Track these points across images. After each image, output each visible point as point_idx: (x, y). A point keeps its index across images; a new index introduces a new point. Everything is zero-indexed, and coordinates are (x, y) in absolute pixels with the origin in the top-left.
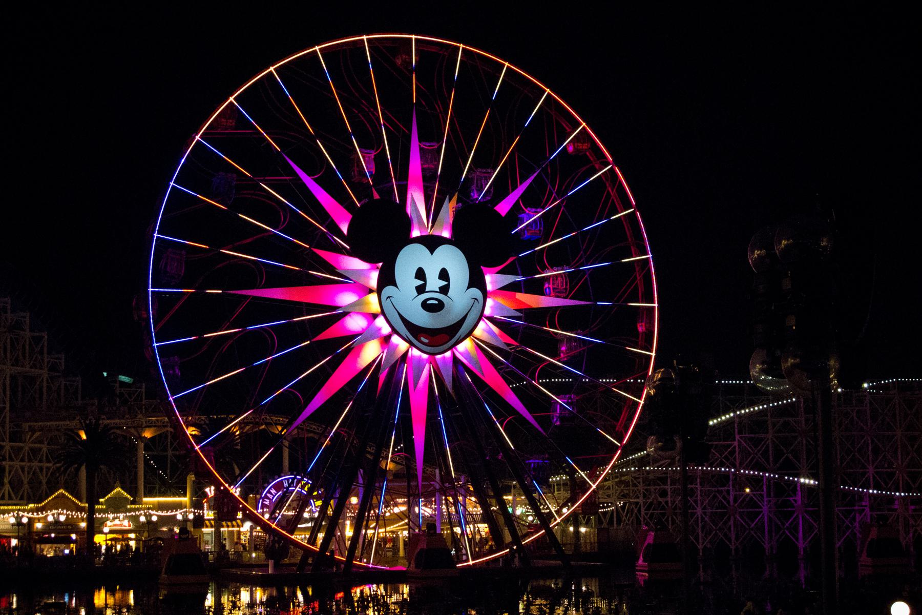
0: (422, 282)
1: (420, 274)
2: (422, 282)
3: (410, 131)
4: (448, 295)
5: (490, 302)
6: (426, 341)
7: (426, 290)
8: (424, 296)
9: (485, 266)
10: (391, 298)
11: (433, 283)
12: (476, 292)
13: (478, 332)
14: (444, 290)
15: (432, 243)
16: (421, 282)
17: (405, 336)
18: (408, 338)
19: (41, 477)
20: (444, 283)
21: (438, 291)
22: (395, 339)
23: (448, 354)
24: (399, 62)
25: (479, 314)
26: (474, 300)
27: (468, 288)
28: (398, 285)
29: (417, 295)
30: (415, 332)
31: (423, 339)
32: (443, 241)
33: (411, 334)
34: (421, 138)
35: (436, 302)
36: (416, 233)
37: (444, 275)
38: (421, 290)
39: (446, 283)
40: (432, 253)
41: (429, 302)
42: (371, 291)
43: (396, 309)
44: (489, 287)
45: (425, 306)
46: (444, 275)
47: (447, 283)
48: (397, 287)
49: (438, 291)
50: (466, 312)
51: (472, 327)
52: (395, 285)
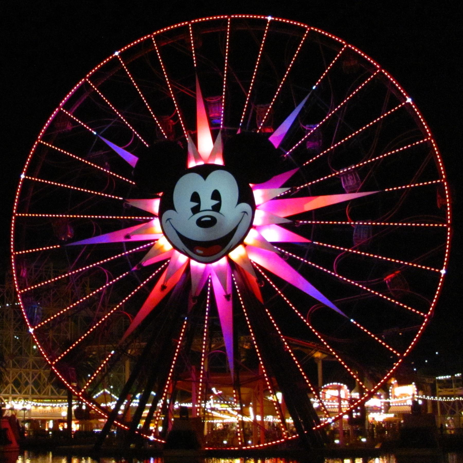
0: (196, 204)
7: (201, 209)
8: (198, 215)
10: (170, 220)
12: (245, 206)
13: (246, 241)
14: (217, 208)
16: (195, 204)
17: (183, 250)
18: (185, 251)
20: (215, 202)
21: (211, 208)
22: (177, 252)
23: (223, 261)
25: (249, 224)
26: (243, 213)
29: (192, 214)
33: (188, 248)
36: (192, 164)
37: (216, 195)
38: (196, 210)
42: (154, 216)
43: (173, 226)
45: (200, 223)
50: (237, 224)
51: (242, 236)
52: (173, 208)
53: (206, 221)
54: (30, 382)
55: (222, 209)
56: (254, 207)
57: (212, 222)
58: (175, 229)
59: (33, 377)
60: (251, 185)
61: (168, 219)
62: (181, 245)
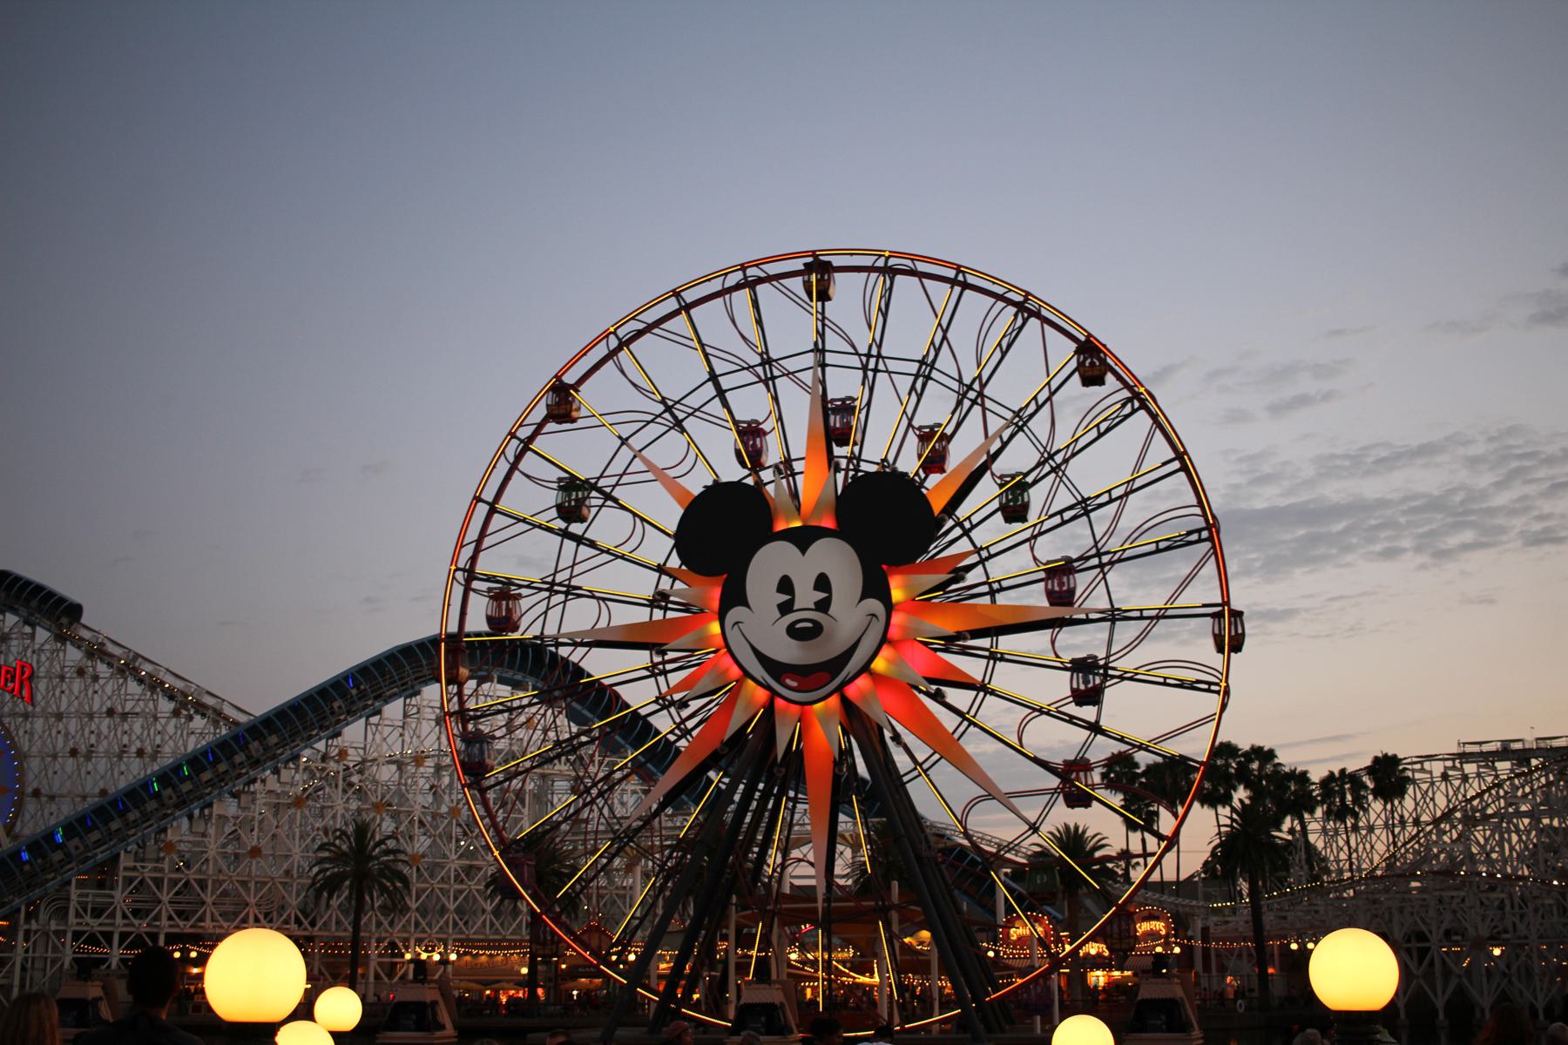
0: (787, 597)
1: (785, 585)
2: (786, 597)
4: (831, 612)
5: (897, 619)
6: (794, 684)
7: (795, 608)
9: (890, 565)
11: (806, 596)
12: (874, 605)
14: (823, 606)
15: (803, 538)
16: (785, 597)
17: (761, 680)
19: (408, 902)
20: (821, 595)
21: (813, 607)
27: (861, 599)
29: (779, 615)
30: (776, 669)
31: (788, 681)
32: (821, 533)
37: (822, 583)
38: (785, 608)
39: (821, 595)
40: (803, 551)
41: (798, 626)
44: (897, 595)
45: (792, 631)
46: (822, 583)
47: (825, 595)
48: (748, 607)
49: (813, 607)
52: (747, 605)
54: (452, 907)
55: (833, 610)
56: (889, 607)
57: (815, 631)
59: (456, 899)
60: (884, 566)
61: (737, 623)
62: (758, 670)
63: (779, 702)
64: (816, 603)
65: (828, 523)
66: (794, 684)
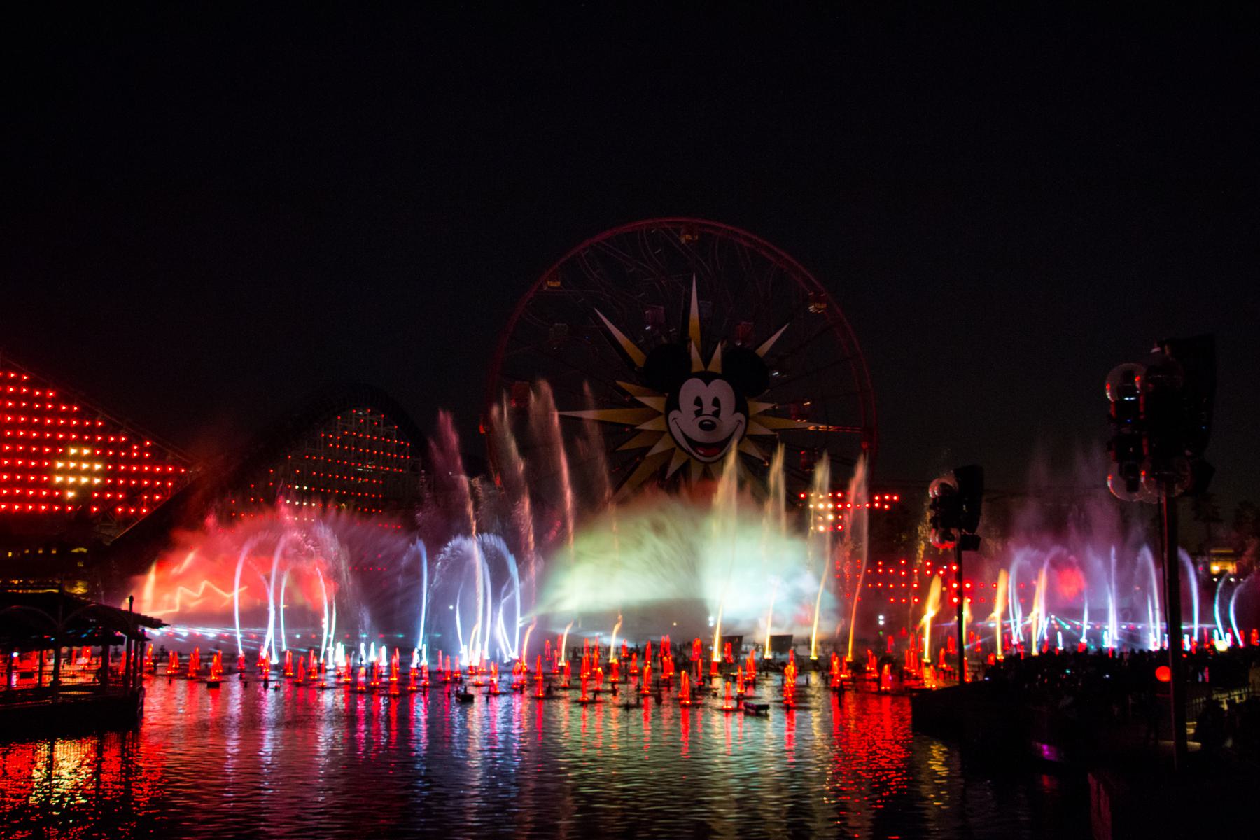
0: (697, 408)
1: (698, 401)
3: (691, 291)
6: (702, 452)
7: (703, 413)
8: (701, 419)
11: (708, 409)
12: (740, 416)
14: (716, 414)
15: (707, 378)
16: (697, 408)
20: (716, 409)
21: (711, 414)
24: (683, 241)
28: (681, 408)
29: (694, 417)
31: (700, 451)
33: (692, 448)
34: (698, 299)
35: (710, 423)
36: (695, 369)
37: (716, 402)
38: (698, 413)
39: (716, 409)
40: (707, 384)
41: (705, 423)
45: (701, 425)
46: (716, 402)
49: (711, 414)
50: (731, 431)
52: (679, 410)
53: (706, 425)
55: (722, 415)
58: (681, 430)
60: (746, 398)
61: (674, 419)
63: (692, 460)
64: (713, 412)
65: (720, 372)
66: (702, 452)
